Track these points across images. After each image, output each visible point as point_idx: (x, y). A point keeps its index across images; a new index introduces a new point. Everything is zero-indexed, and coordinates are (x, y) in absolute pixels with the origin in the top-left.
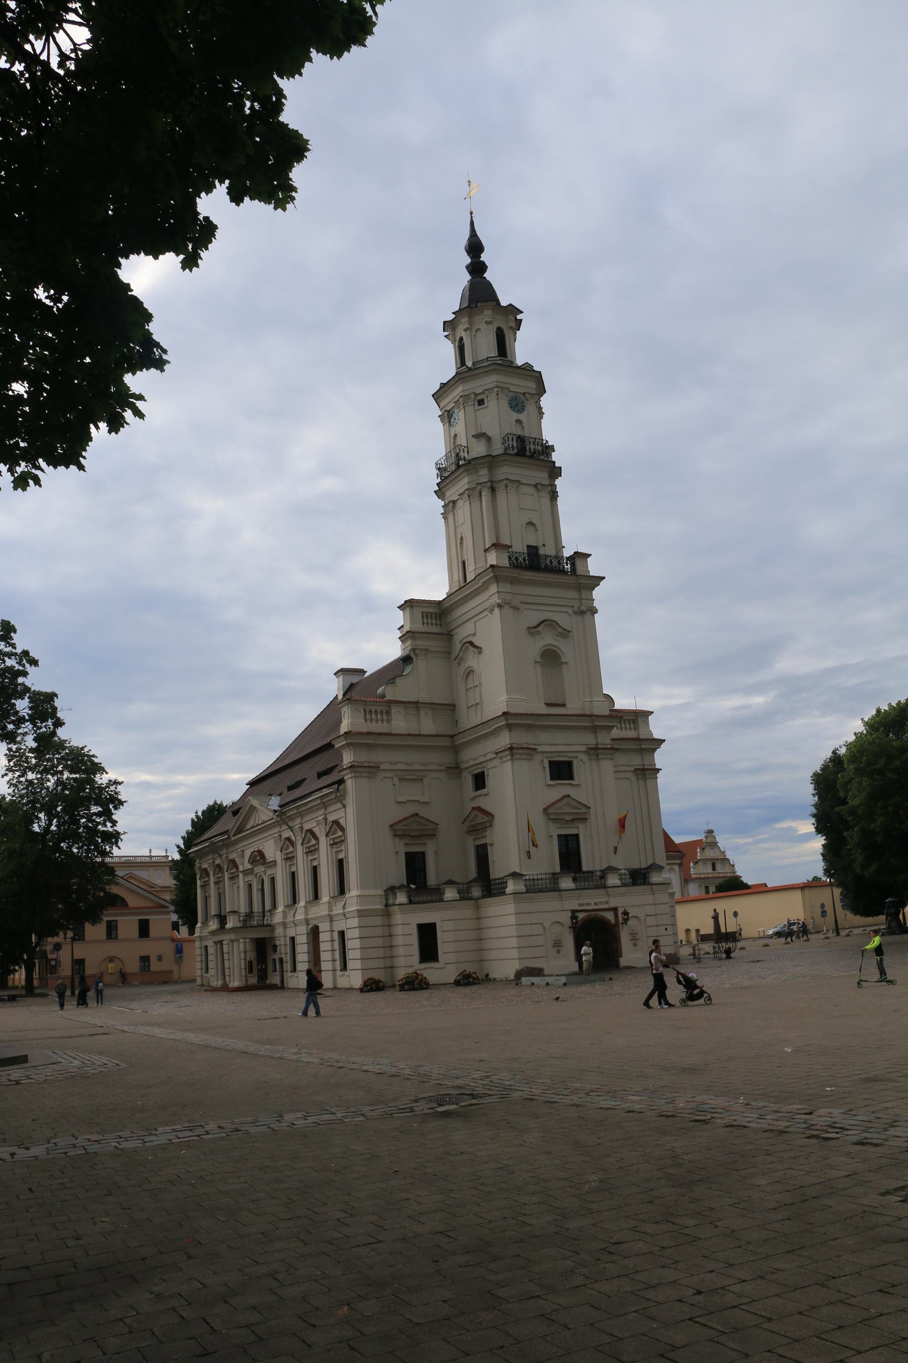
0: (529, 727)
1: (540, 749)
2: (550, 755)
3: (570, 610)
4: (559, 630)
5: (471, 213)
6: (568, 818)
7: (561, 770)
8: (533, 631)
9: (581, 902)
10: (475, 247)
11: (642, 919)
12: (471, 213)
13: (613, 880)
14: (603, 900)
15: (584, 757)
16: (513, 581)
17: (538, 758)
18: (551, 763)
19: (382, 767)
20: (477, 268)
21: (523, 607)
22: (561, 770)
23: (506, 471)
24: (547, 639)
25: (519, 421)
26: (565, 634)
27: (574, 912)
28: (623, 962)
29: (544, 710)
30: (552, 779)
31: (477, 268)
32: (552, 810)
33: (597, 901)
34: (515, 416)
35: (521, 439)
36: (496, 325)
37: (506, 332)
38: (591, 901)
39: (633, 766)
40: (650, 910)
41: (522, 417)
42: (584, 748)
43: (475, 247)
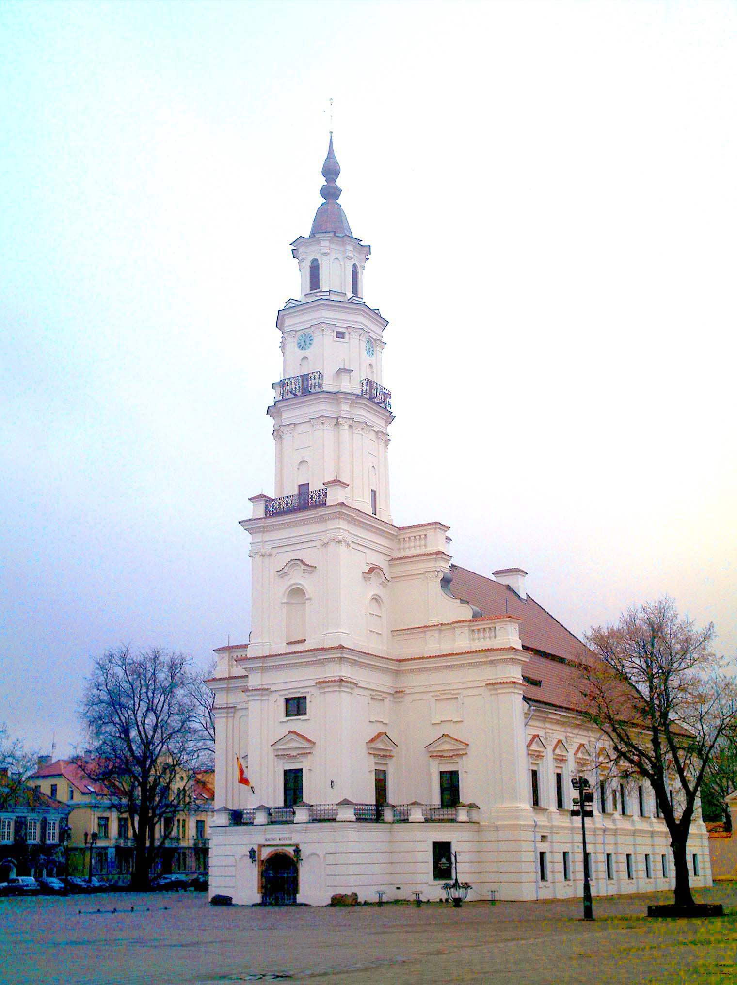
0: (263, 669)
1: (273, 688)
2: (283, 693)
3: (317, 543)
4: (303, 567)
5: (331, 133)
6: (294, 753)
7: (296, 706)
8: (282, 573)
9: (268, 836)
10: (331, 171)
11: (321, 856)
12: (331, 133)
13: (301, 815)
14: (288, 836)
15: (313, 691)
16: (264, 530)
17: (273, 697)
18: (288, 700)
19: (238, 707)
20: (331, 193)
21: (275, 551)
22: (296, 706)
23: (288, 416)
24: (297, 578)
25: (305, 358)
26: (310, 568)
27: (261, 846)
28: (300, 898)
29: (284, 649)
30: (287, 715)
31: (331, 193)
32: (277, 747)
33: (281, 836)
34: (303, 353)
35: (305, 378)
36: (311, 258)
37: (320, 262)
38: (281, 837)
39: (484, 680)
40: (331, 847)
41: (307, 353)
42: (312, 683)
43: (331, 171)
